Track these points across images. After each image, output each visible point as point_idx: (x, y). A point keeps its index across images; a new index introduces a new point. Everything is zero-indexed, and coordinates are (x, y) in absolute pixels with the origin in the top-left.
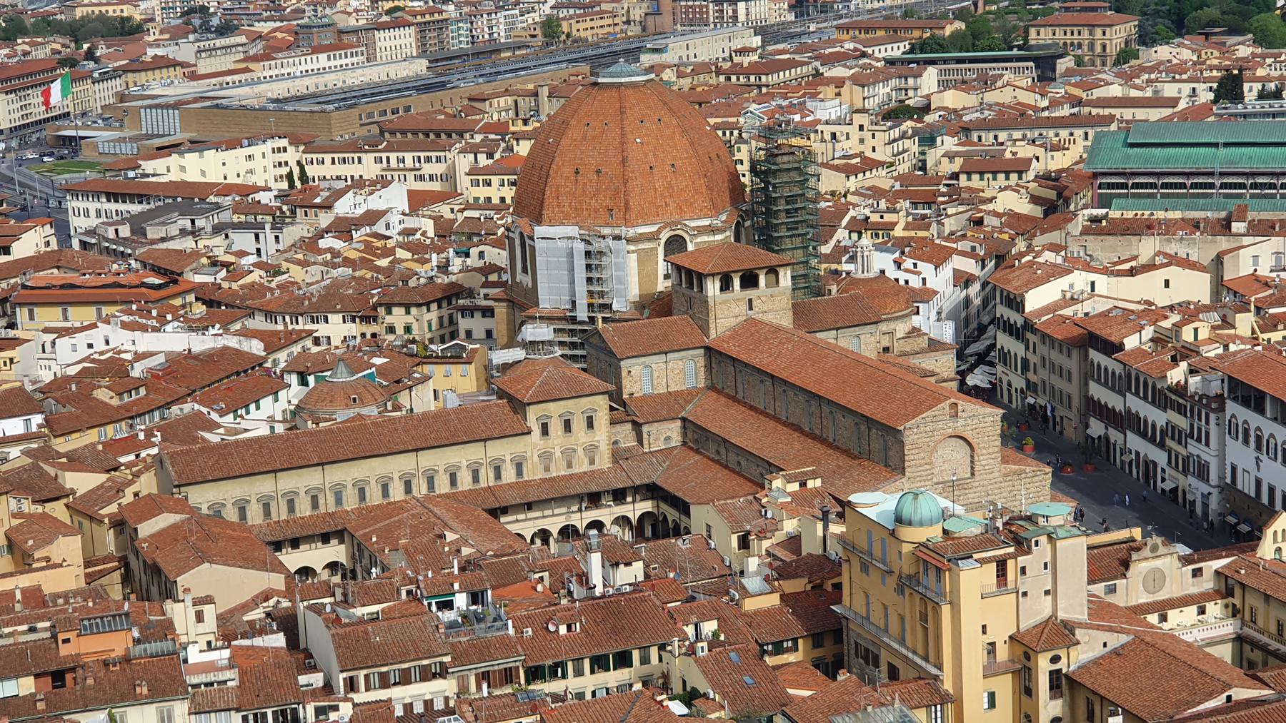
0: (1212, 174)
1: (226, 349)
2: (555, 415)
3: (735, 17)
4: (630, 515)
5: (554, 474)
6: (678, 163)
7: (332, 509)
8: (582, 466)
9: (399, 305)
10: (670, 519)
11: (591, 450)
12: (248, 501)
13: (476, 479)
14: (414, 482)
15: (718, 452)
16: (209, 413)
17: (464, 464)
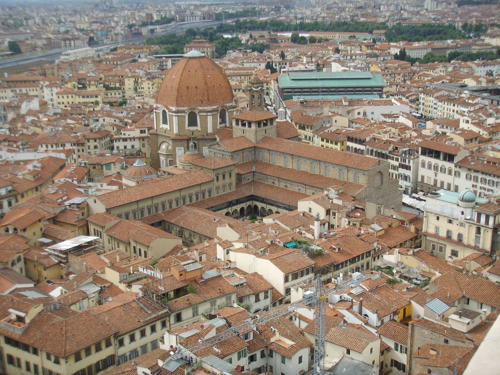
0: (319, 88)
1: (51, 157)
2: (221, 173)
3: (70, 46)
4: (245, 207)
5: (220, 194)
6: (221, 84)
7: (155, 214)
8: (228, 191)
9: (92, 139)
10: (259, 207)
11: (230, 185)
12: (129, 213)
13: (197, 199)
14: (179, 201)
15: (273, 183)
16: (73, 181)
17: (194, 193)
